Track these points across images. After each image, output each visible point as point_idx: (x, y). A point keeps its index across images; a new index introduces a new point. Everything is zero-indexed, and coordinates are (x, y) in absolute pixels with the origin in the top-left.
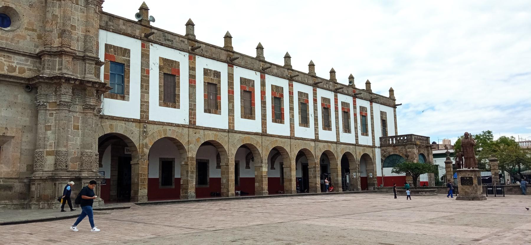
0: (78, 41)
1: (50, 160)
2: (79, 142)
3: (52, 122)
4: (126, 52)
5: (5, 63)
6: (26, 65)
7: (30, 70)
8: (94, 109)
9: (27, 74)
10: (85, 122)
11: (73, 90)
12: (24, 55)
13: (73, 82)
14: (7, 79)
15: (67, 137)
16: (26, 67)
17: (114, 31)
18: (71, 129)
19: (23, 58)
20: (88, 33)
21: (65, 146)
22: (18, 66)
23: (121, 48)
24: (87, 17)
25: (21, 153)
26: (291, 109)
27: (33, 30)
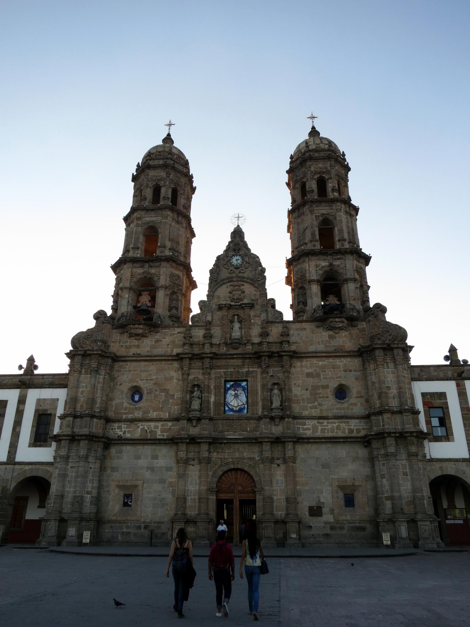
0: (394, 398)
1: (388, 504)
2: (409, 487)
3: (385, 472)
4: (443, 395)
5: (346, 427)
6: (361, 426)
7: (364, 429)
8: (417, 455)
9: (362, 433)
10: (411, 468)
11: (396, 441)
12: (358, 418)
13: (393, 435)
14: (349, 440)
15: (398, 483)
16: (361, 427)
17: (427, 380)
18: (401, 476)
19: (358, 421)
20: (401, 390)
21: (398, 492)
22: (355, 428)
23: (437, 393)
24: (398, 377)
25: (367, 498)
27: (362, 397)
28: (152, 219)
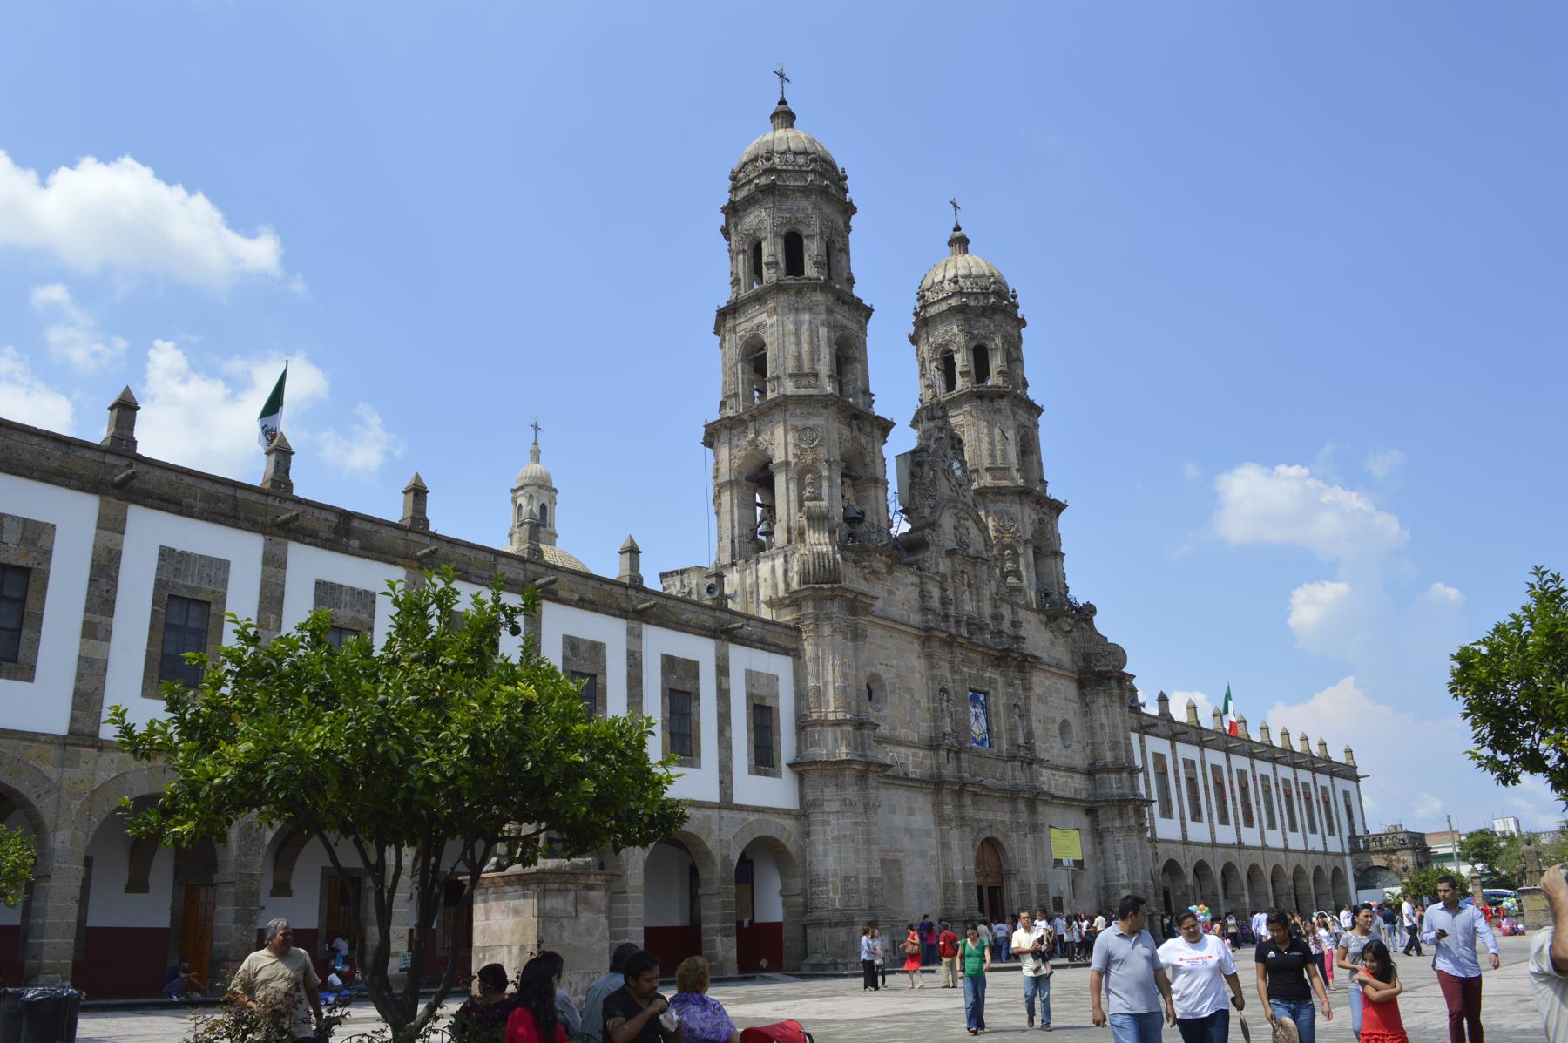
3: (1121, 850)
9: (1084, 795)
26: (1258, 803)
28: (845, 322)
